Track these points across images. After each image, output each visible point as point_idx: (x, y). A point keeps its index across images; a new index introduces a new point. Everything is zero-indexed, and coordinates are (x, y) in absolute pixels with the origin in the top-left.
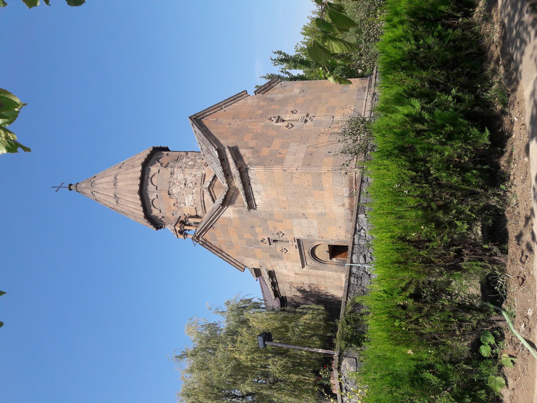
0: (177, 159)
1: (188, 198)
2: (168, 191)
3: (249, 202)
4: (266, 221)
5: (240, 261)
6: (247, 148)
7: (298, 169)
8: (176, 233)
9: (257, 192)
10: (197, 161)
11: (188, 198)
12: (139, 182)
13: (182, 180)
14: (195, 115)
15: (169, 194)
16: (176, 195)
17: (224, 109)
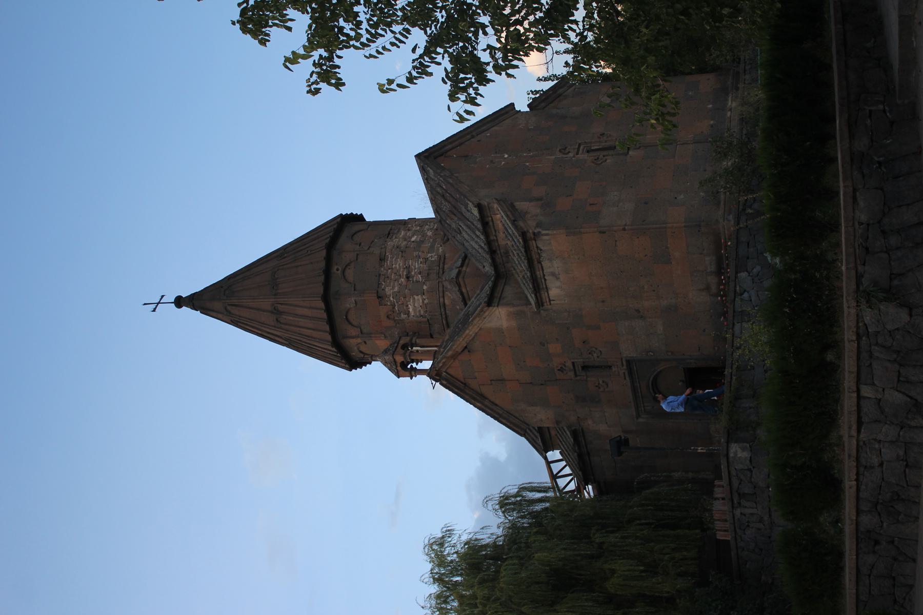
0: (389, 234)
1: (414, 302)
2: (376, 291)
3: (538, 295)
4: (568, 328)
6: (531, 200)
7: (626, 227)
9: (553, 274)
10: (426, 233)
11: (414, 302)
12: (322, 278)
13: (402, 270)
14: (426, 150)
15: (379, 297)
16: (392, 299)
17: (479, 137)
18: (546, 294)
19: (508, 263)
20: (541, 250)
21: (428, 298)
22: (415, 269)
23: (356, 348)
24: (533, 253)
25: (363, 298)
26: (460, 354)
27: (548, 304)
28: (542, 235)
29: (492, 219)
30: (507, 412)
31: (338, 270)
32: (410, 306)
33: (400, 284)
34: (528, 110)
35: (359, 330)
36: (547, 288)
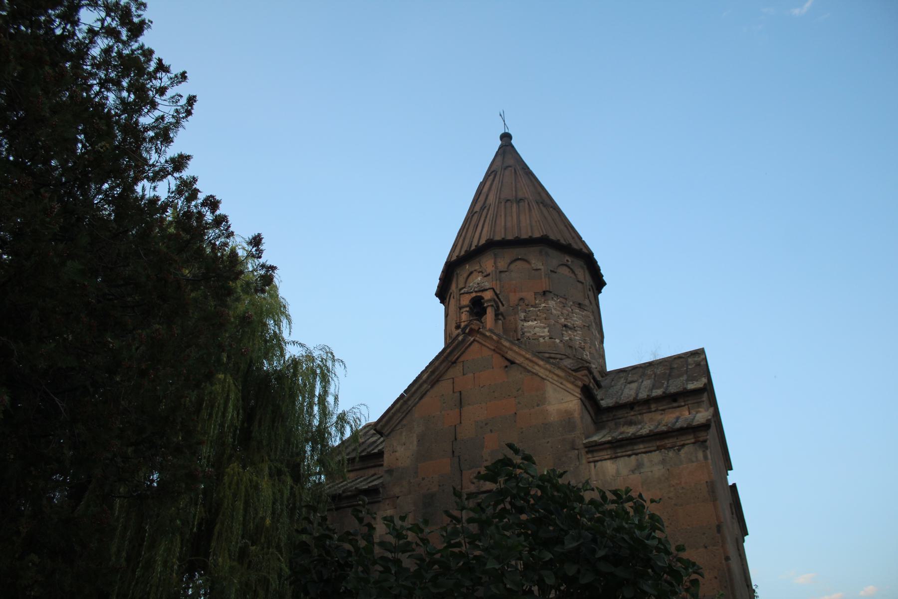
1: (540, 327)
2: (551, 291)
3: (607, 446)
5: (404, 422)
8: (476, 292)
9: (639, 466)
11: (540, 327)
13: (572, 322)
15: (544, 293)
16: (544, 305)
18: (606, 457)
19: (616, 424)
20: (679, 450)
21: (545, 342)
22: (574, 336)
23: (477, 267)
24: (675, 440)
25: (543, 276)
26: (503, 356)
27: (591, 460)
28: (704, 451)
29: (679, 407)
30: (409, 411)
31: (567, 261)
32: (536, 322)
33: (559, 316)
34: (730, 483)
35: (503, 270)
36: (616, 457)
